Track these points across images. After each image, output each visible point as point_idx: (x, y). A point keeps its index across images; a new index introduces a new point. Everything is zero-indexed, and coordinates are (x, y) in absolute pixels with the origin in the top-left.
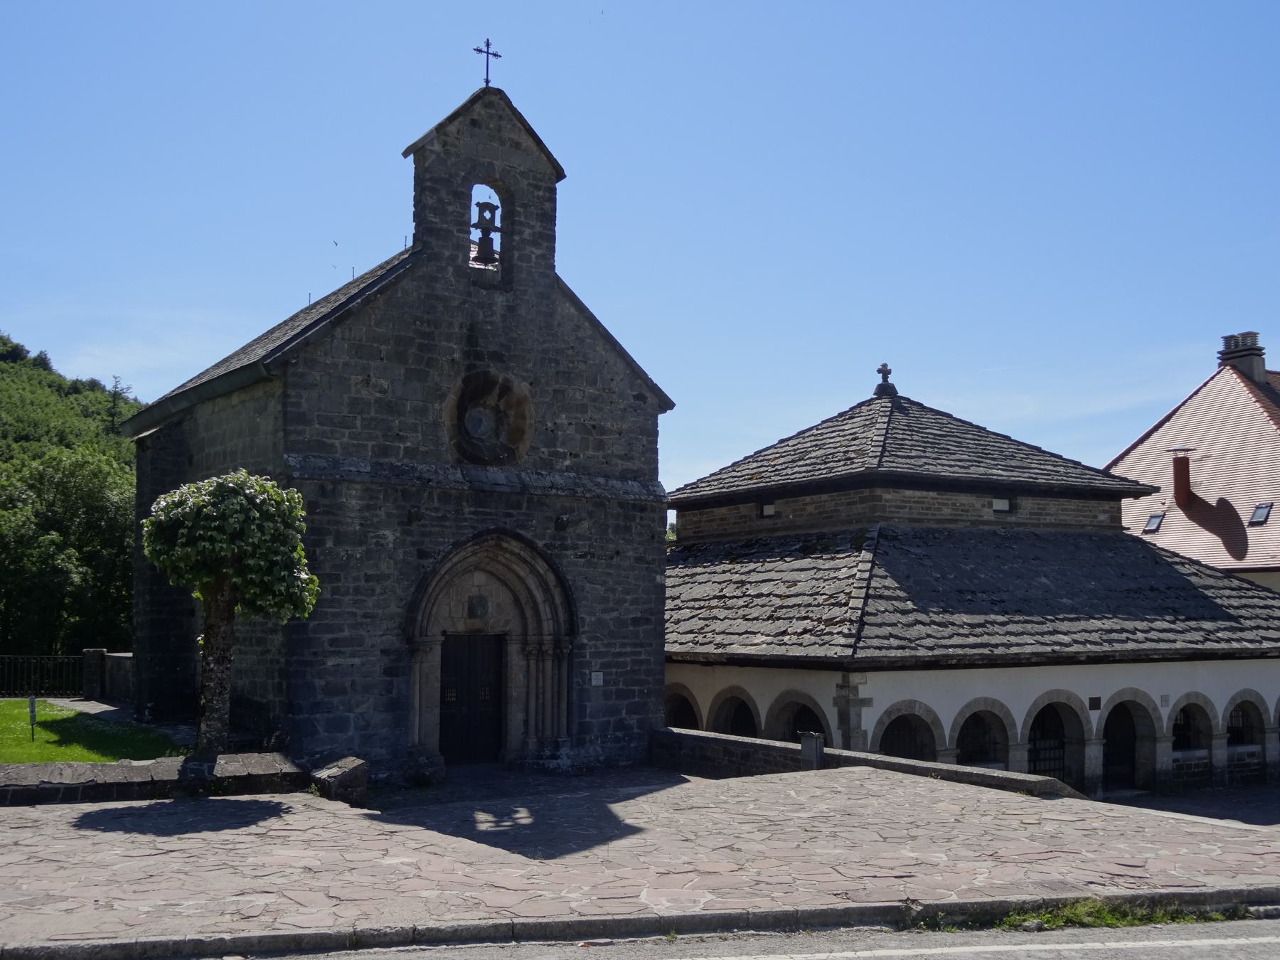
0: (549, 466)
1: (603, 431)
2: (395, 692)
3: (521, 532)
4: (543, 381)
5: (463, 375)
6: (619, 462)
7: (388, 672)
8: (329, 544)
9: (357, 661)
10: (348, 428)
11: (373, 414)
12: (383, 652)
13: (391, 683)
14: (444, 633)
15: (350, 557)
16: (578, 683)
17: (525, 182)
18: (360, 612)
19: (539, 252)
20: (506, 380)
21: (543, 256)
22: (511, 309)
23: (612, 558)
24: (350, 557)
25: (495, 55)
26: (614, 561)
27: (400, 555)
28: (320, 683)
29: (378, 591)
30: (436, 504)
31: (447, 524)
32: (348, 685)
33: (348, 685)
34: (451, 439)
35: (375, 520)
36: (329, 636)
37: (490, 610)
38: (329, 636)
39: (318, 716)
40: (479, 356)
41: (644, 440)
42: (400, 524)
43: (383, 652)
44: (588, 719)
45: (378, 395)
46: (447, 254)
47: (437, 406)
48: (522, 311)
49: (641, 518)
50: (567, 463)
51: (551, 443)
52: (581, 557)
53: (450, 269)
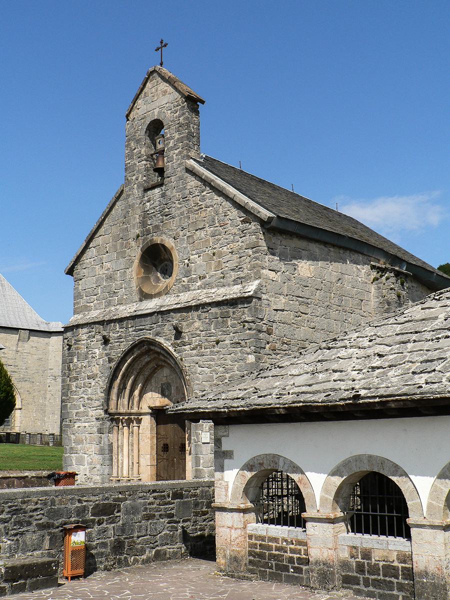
0: (187, 289)
1: (221, 255)
2: (102, 442)
3: (158, 339)
4: (181, 233)
5: (141, 246)
6: (232, 273)
7: (100, 431)
8: (75, 360)
9: (86, 424)
10: (96, 295)
11: (104, 284)
12: (97, 419)
13: (101, 438)
14: (150, 408)
15: (82, 366)
16: (194, 440)
17: (169, 112)
18: (86, 397)
19: (176, 152)
20: (162, 240)
21: (180, 153)
22: (163, 195)
23: (214, 346)
24: (82, 366)
25: (165, 46)
26: (216, 349)
27: (101, 361)
28: (73, 437)
29: (93, 384)
30: (118, 329)
31: (122, 340)
32: (84, 438)
33: (84, 438)
34: (137, 287)
35: (92, 343)
36: (76, 411)
37: (172, 392)
38: (76, 411)
39: (73, 455)
40: (148, 232)
41: (250, 252)
42: (102, 345)
43: (97, 419)
44: (201, 467)
45: (106, 272)
46: (134, 178)
47: (130, 270)
48: (168, 193)
49: (234, 313)
50: (199, 283)
51: (187, 274)
52: (193, 349)
53: (136, 186)
